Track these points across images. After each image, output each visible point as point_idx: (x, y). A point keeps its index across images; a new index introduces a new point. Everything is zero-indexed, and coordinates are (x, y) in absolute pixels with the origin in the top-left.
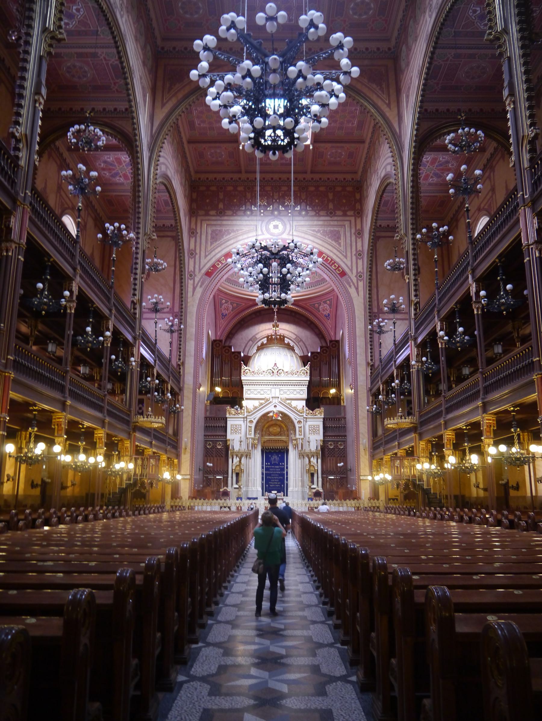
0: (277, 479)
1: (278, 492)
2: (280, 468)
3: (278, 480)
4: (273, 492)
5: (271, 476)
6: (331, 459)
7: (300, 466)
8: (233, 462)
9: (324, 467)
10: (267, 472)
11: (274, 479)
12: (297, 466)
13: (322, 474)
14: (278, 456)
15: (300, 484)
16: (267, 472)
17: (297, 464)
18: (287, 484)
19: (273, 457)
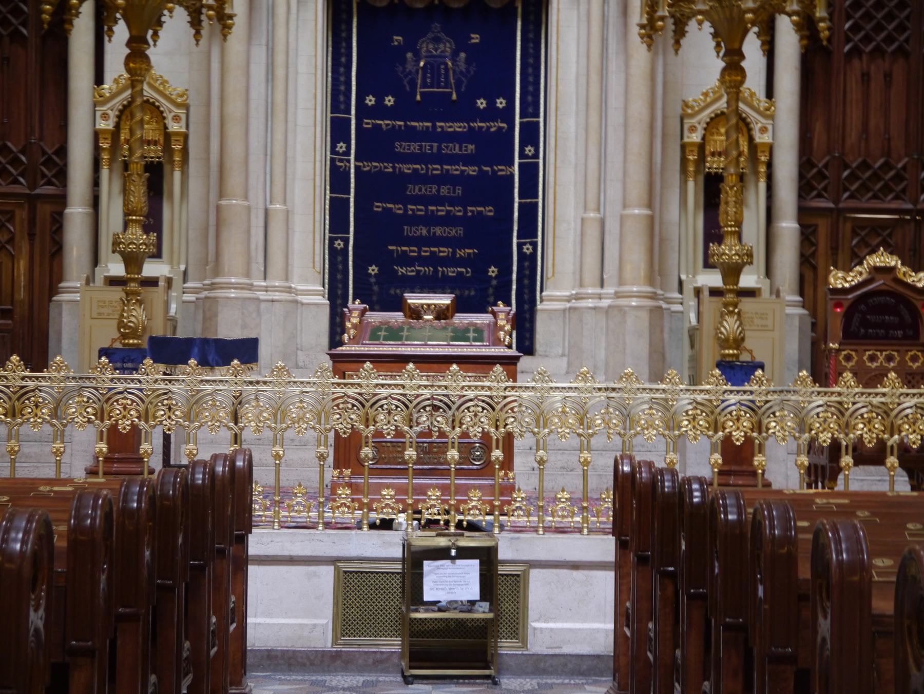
0: (449, 220)
1: (461, 306)
2: (471, 136)
3: (456, 232)
4: (414, 299)
5: (406, 200)
6: (876, 84)
7: (639, 108)
8: (99, 79)
9: (819, 127)
10: (367, 167)
11: (430, 220)
12: (615, 117)
13: (805, 187)
14: (461, 44)
15: (637, 257)
16: (367, 167)
17: (615, 101)
18: (529, 263)
19: (426, 47)
